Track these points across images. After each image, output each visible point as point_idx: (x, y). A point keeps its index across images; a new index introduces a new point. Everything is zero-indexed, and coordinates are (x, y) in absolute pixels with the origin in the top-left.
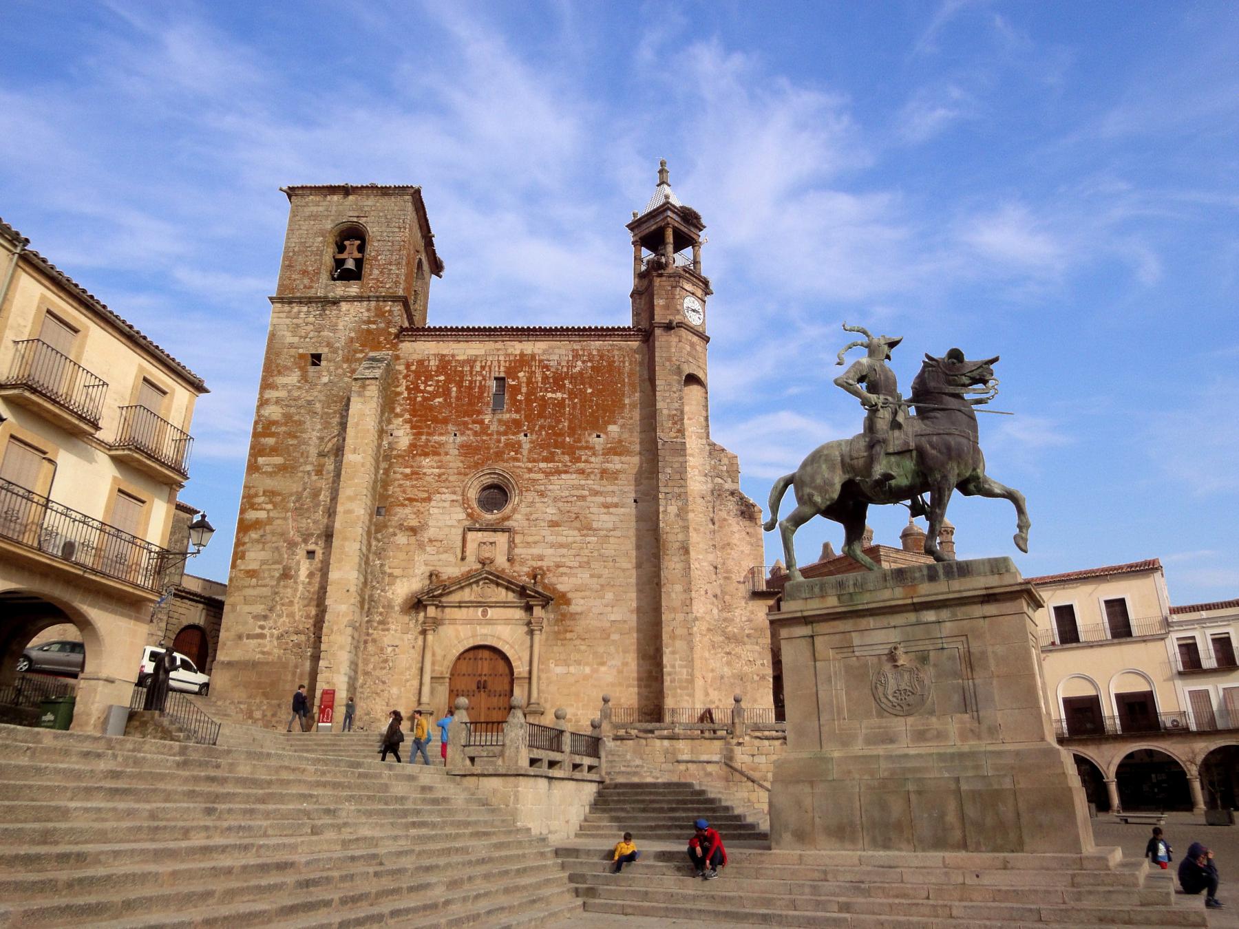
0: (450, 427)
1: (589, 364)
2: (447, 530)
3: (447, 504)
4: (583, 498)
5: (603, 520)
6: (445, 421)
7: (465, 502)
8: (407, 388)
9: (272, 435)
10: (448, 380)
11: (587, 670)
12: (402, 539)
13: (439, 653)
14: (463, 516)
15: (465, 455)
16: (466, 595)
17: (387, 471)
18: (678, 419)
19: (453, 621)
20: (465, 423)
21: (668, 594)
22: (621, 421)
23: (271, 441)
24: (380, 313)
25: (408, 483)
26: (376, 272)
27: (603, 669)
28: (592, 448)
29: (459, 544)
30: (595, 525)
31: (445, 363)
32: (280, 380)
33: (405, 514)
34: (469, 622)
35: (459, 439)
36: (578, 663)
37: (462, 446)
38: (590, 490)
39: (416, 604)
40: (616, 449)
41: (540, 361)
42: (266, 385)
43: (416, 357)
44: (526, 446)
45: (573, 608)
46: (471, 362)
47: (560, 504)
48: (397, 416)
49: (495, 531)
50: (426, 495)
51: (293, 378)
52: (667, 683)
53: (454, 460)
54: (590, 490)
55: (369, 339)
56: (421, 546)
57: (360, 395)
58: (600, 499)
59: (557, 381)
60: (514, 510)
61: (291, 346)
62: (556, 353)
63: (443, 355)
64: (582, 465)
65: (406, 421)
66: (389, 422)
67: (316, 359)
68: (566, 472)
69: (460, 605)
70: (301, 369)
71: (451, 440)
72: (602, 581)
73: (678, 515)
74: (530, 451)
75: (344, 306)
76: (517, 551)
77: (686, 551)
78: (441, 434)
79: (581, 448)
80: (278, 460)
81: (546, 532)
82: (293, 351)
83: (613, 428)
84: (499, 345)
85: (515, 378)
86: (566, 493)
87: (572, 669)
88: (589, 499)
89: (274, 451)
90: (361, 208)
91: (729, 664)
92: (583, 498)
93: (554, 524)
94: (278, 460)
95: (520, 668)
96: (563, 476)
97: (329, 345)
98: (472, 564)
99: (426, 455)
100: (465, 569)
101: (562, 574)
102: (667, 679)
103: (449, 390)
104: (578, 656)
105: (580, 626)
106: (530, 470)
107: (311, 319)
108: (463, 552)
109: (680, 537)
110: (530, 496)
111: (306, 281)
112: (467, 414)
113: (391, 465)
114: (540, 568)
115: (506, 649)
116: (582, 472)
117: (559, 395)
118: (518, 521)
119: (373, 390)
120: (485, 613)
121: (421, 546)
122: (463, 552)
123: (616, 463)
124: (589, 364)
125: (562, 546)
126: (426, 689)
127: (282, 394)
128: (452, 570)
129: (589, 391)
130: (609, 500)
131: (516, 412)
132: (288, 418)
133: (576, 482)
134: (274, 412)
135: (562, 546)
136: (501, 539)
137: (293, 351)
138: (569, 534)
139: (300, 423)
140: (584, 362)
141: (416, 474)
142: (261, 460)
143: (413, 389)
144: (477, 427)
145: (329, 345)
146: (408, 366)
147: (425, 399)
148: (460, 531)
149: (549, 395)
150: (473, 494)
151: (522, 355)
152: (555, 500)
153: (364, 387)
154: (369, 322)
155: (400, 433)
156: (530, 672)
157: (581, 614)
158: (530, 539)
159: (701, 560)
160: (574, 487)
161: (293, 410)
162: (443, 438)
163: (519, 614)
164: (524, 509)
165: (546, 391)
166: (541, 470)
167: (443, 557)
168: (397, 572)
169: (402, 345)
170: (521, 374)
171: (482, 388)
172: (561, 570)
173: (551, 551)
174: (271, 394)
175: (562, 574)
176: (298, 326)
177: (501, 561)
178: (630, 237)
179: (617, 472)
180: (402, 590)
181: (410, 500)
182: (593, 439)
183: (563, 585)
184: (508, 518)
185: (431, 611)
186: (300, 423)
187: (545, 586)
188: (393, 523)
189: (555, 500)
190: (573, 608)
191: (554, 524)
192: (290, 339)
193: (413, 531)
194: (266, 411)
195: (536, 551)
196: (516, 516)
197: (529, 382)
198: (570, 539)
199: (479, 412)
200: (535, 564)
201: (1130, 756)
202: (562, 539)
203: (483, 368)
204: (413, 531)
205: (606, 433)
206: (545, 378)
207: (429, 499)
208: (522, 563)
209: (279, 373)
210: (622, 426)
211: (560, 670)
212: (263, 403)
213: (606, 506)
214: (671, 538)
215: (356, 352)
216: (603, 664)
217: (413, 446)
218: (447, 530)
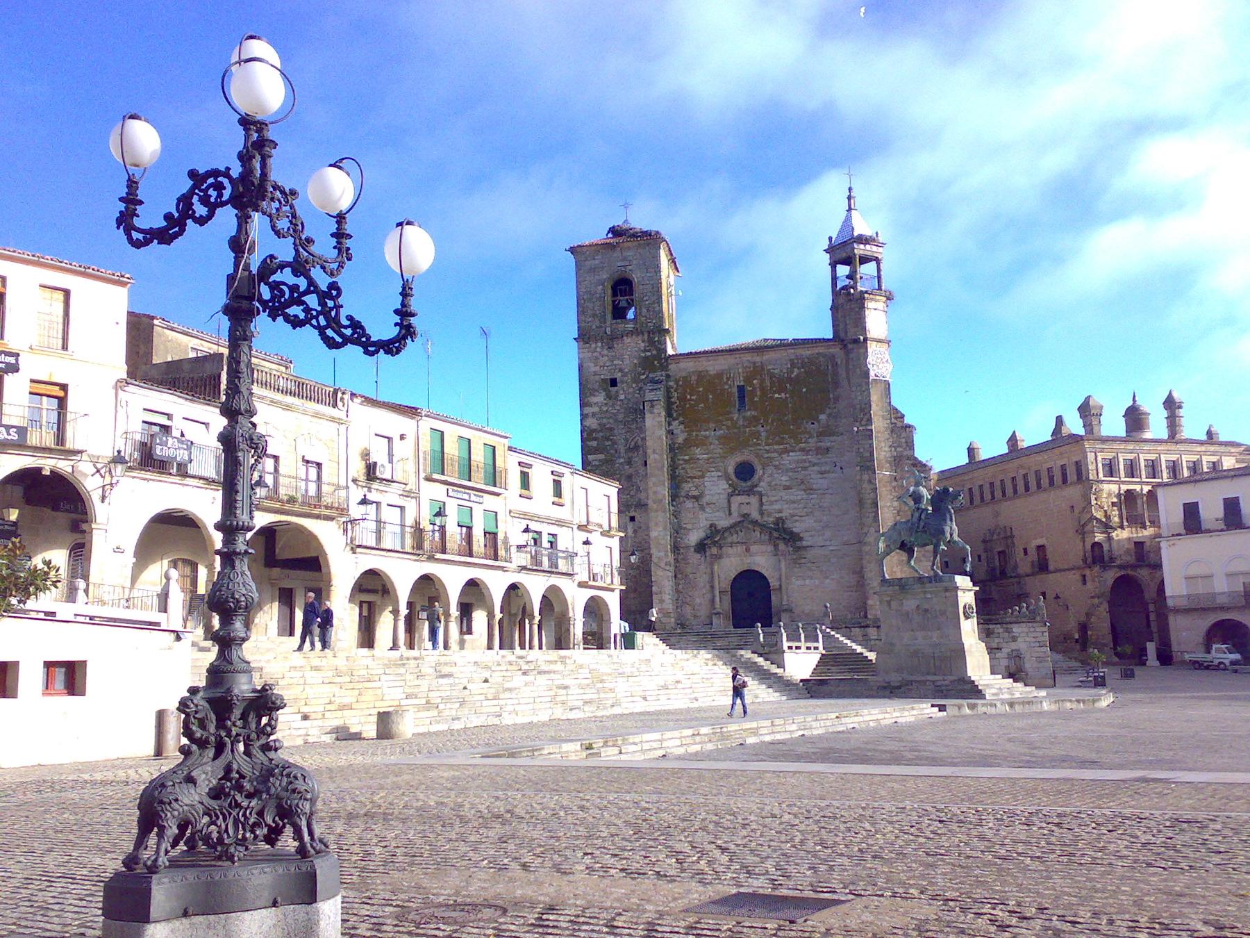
0: (712, 425)
2: (717, 497)
4: (805, 468)
5: (819, 482)
6: (707, 421)
7: (728, 478)
9: (595, 439)
12: (689, 504)
13: (723, 577)
15: (723, 444)
17: (673, 460)
19: (729, 556)
22: (828, 411)
23: (594, 444)
24: (651, 342)
26: (644, 310)
27: (827, 581)
28: (809, 433)
29: (726, 505)
31: (701, 376)
32: (593, 400)
33: (686, 487)
35: (718, 433)
36: (811, 578)
37: (720, 438)
39: (701, 547)
40: (827, 432)
45: (805, 543)
46: (719, 375)
48: (675, 420)
51: (600, 398)
53: (718, 449)
56: (702, 508)
58: (816, 468)
59: (780, 383)
60: (760, 480)
61: (595, 374)
62: (777, 363)
65: (681, 423)
66: (670, 424)
69: (731, 545)
70: (604, 390)
71: (710, 434)
74: (767, 438)
75: (627, 340)
79: (803, 433)
80: (602, 456)
81: (783, 493)
82: (597, 378)
83: (823, 417)
85: (752, 385)
89: (596, 451)
90: (624, 259)
93: (787, 488)
95: (773, 583)
97: (621, 370)
98: (735, 518)
100: (732, 521)
103: (707, 399)
104: (810, 573)
105: (810, 554)
106: (768, 452)
107: (605, 352)
110: (769, 470)
111: (597, 323)
113: (675, 455)
114: (781, 518)
115: (764, 572)
116: (802, 450)
117: (783, 395)
118: (762, 487)
119: (660, 410)
120: (748, 550)
121: (702, 508)
123: (826, 443)
126: (717, 599)
127: (596, 409)
128: (723, 523)
131: (756, 410)
134: (592, 423)
136: (754, 500)
137: (597, 378)
138: (797, 494)
139: (611, 429)
141: (693, 460)
143: (682, 399)
144: (729, 423)
145: (621, 370)
146: (677, 382)
148: (725, 496)
150: (731, 470)
152: (787, 471)
153: (652, 406)
154: (645, 351)
160: (798, 462)
161: (605, 421)
163: (770, 548)
164: (766, 479)
165: (775, 392)
166: (775, 451)
168: (689, 526)
171: (730, 394)
174: (587, 410)
176: (597, 358)
177: (755, 515)
179: (828, 449)
180: (693, 538)
181: (692, 478)
182: (809, 426)
183: (797, 528)
185: (714, 550)
187: (785, 529)
188: (683, 494)
189: (787, 471)
191: (787, 488)
192: (593, 369)
193: (696, 498)
194: (588, 422)
195: (777, 507)
197: (762, 389)
199: (731, 413)
202: (792, 498)
203: (728, 379)
204: (696, 498)
205: (819, 422)
206: (772, 382)
207: (703, 477)
208: (769, 515)
209: (591, 395)
210: (829, 415)
211: (799, 583)
215: (640, 374)
218: (717, 497)
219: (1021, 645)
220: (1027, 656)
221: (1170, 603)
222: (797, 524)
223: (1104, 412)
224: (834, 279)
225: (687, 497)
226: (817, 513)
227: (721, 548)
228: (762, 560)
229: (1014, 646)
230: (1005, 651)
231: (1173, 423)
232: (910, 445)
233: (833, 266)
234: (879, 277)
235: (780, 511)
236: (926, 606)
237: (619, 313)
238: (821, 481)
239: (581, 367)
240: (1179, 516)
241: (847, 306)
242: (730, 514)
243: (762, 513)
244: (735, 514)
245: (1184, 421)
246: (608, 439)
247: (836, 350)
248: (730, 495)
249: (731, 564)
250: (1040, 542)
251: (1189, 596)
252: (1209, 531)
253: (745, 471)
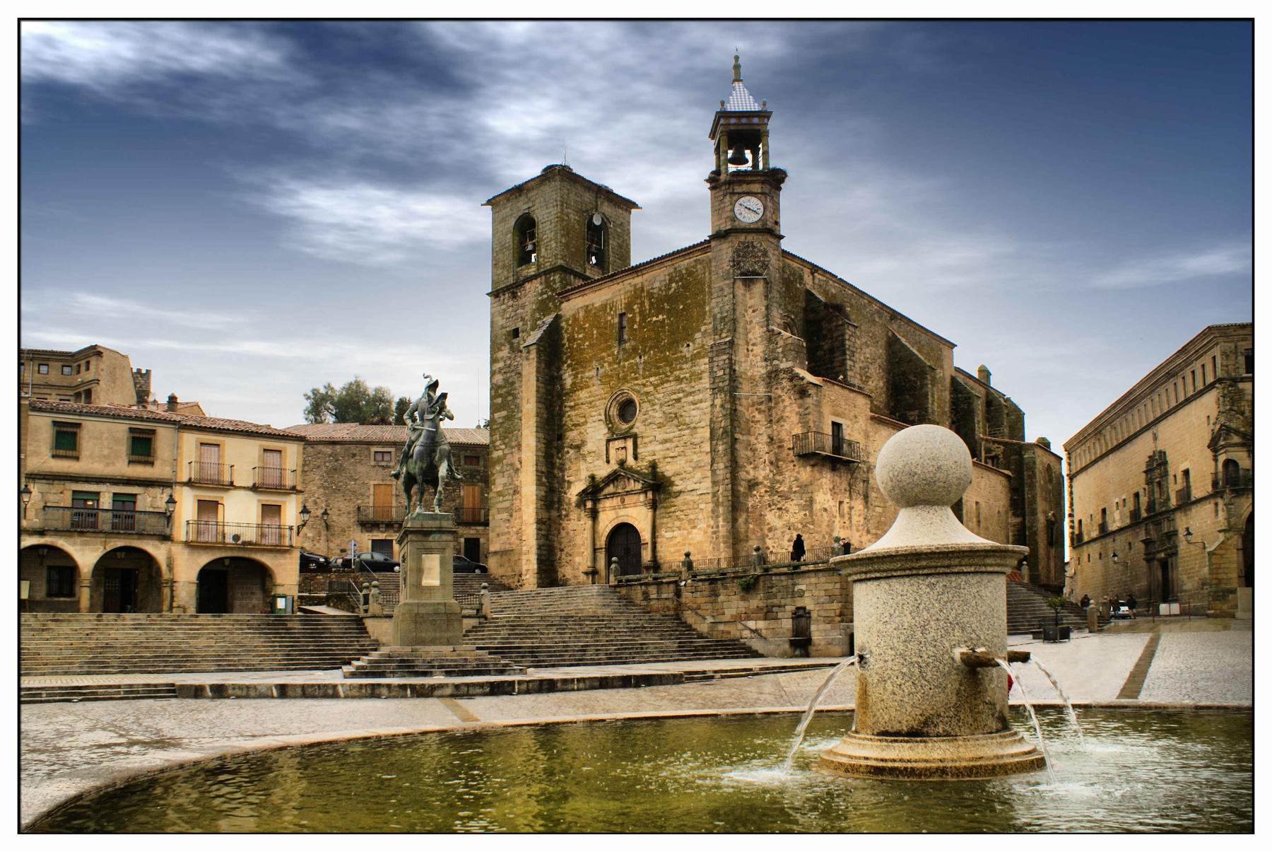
6: (591, 361)
7: (608, 420)
8: (568, 340)
10: (591, 326)
14: (606, 431)
16: (611, 489)
20: (603, 358)
23: (499, 400)
24: (548, 285)
25: (573, 413)
27: (695, 531)
32: (500, 354)
33: (572, 436)
34: (614, 508)
36: (679, 528)
42: (494, 361)
43: (571, 313)
45: (675, 489)
47: (665, 408)
49: (625, 438)
50: (582, 420)
51: (505, 352)
55: (543, 308)
56: (584, 457)
57: (527, 359)
61: (503, 327)
67: (516, 333)
75: (528, 286)
80: (504, 413)
84: (617, 287)
87: (676, 533)
91: (780, 517)
94: (504, 413)
97: (523, 319)
98: (614, 466)
99: (582, 389)
104: (677, 523)
106: (644, 385)
108: (608, 458)
112: (603, 350)
118: (638, 428)
122: (608, 458)
125: (666, 441)
128: (603, 471)
132: (506, 380)
135: (666, 441)
138: (671, 432)
142: (496, 415)
145: (523, 319)
147: (579, 345)
150: (614, 412)
152: (661, 405)
155: (566, 376)
167: (597, 463)
169: (564, 305)
173: (660, 447)
177: (631, 461)
181: (575, 425)
184: (632, 427)
186: (513, 383)
190: (675, 489)
191: (660, 426)
192: (501, 322)
198: (671, 435)
200: (650, 458)
209: (500, 350)
211: (668, 535)
212: (493, 373)
216: (695, 527)
217: (574, 384)
219: (808, 603)
220: (814, 615)
225: (571, 447)
226: (688, 452)
227: (596, 501)
228: (638, 515)
229: (799, 603)
230: (790, 608)
237: (524, 259)
239: (492, 322)
242: (608, 462)
244: (613, 461)
246: (509, 393)
248: (608, 441)
249: (609, 518)
253: (627, 409)
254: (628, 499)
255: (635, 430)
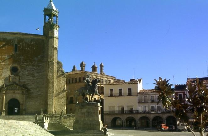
1: (35, 43)
3: (6, 71)
4: (33, 71)
11: (34, 103)
18: (52, 56)
21: (49, 90)
27: (36, 103)
30: (35, 76)
38: (34, 69)
41: (25, 41)
44: (22, 60)
45: (31, 92)
46: (11, 40)
47: (29, 72)
52: (49, 106)
54: (34, 69)
58: (36, 71)
63: (4, 38)
64: (33, 64)
68: (30, 65)
72: (37, 87)
73: (52, 76)
76: (21, 80)
77: (53, 82)
78: (4, 56)
81: (26, 77)
83: (39, 57)
86: (30, 69)
87: (31, 103)
88: (34, 71)
92: (33, 71)
93: (27, 75)
95: (21, 103)
96: (29, 66)
101: (29, 85)
102: (49, 105)
106: (23, 64)
109: (52, 80)
110: (23, 70)
114: (25, 84)
115: (18, 99)
116: (33, 65)
117: (28, 49)
124: (35, 43)
125: (29, 80)
129: (35, 48)
130: (38, 71)
133: (32, 67)
135: (29, 80)
136: (17, 78)
140: (34, 42)
149: (27, 49)
151: (21, 39)
152: (28, 71)
156: (23, 104)
157: (32, 93)
158: (23, 78)
159: (55, 84)
162: (5, 57)
170: (21, 44)
172: (29, 84)
175: (29, 85)
177: (17, 82)
178: (44, 13)
183: (30, 87)
184: (18, 74)
190: (31, 92)
191: (27, 75)
195: (24, 81)
196: (20, 74)
198: (30, 79)
201: (129, 117)
202: (29, 78)
208: (22, 83)
211: (28, 103)
213: (37, 72)
214: (50, 80)
221: (105, 113)
222: (29, 86)
223: (86, 66)
224: (45, 19)
228: (18, 96)
231: (101, 70)
232: (61, 68)
233: (45, 15)
234: (57, 21)
235: (25, 82)
236: (89, 111)
238: (37, 75)
240: (109, 92)
241: (49, 27)
243: (19, 82)
245: (103, 70)
247: (44, 38)
250: (72, 96)
251: (109, 111)
252: (115, 96)
254: (16, 92)
255: (19, 75)
